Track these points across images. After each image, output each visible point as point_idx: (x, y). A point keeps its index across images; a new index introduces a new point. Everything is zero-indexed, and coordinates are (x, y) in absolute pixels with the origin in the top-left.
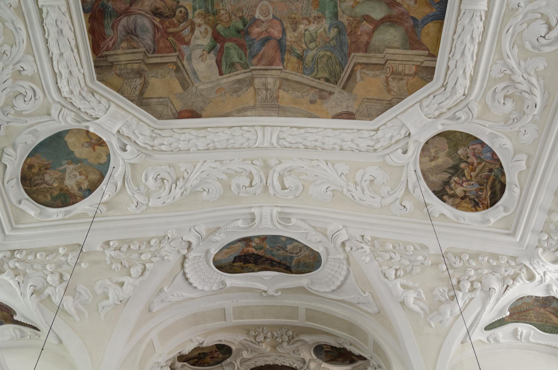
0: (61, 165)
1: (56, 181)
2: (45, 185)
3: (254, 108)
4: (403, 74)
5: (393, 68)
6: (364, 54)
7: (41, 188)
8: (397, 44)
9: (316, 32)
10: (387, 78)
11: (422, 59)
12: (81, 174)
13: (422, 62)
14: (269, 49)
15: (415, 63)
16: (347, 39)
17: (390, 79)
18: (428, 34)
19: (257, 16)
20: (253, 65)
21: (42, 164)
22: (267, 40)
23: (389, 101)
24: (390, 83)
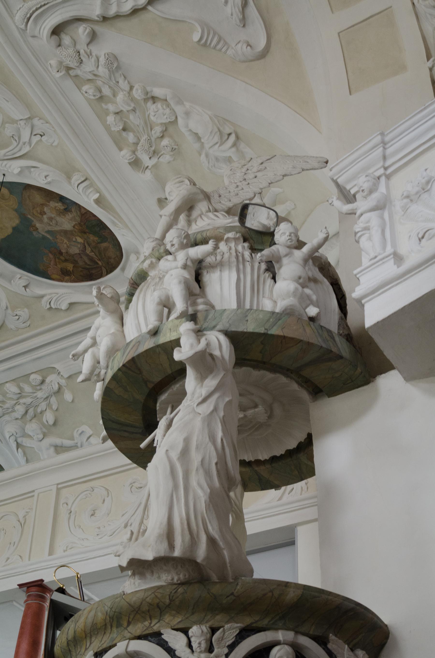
0: (44, 238)
1: (74, 240)
2: (88, 251)
7: (97, 256)
12: (43, 213)
21: (55, 259)
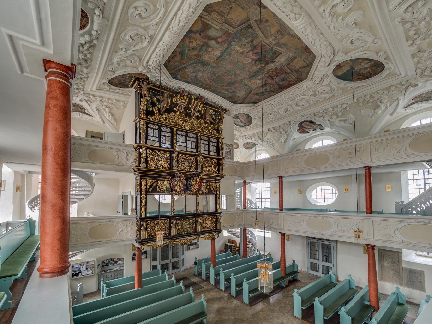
3: (289, 34)
4: (219, 14)
5: (222, 18)
6: (228, 31)
8: (213, 29)
9: (238, 47)
10: (227, 16)
11: (207, 17)
13: (207, 15)
14: (259, 50)
15: (210, 16)
16: (230, 39)
17: (226, 14)
18: (198, 27)
19: (250, 61)
20: (269, 48)
22: (256, 53)
23: (235, 2)
24: (228, 12)
